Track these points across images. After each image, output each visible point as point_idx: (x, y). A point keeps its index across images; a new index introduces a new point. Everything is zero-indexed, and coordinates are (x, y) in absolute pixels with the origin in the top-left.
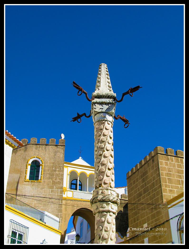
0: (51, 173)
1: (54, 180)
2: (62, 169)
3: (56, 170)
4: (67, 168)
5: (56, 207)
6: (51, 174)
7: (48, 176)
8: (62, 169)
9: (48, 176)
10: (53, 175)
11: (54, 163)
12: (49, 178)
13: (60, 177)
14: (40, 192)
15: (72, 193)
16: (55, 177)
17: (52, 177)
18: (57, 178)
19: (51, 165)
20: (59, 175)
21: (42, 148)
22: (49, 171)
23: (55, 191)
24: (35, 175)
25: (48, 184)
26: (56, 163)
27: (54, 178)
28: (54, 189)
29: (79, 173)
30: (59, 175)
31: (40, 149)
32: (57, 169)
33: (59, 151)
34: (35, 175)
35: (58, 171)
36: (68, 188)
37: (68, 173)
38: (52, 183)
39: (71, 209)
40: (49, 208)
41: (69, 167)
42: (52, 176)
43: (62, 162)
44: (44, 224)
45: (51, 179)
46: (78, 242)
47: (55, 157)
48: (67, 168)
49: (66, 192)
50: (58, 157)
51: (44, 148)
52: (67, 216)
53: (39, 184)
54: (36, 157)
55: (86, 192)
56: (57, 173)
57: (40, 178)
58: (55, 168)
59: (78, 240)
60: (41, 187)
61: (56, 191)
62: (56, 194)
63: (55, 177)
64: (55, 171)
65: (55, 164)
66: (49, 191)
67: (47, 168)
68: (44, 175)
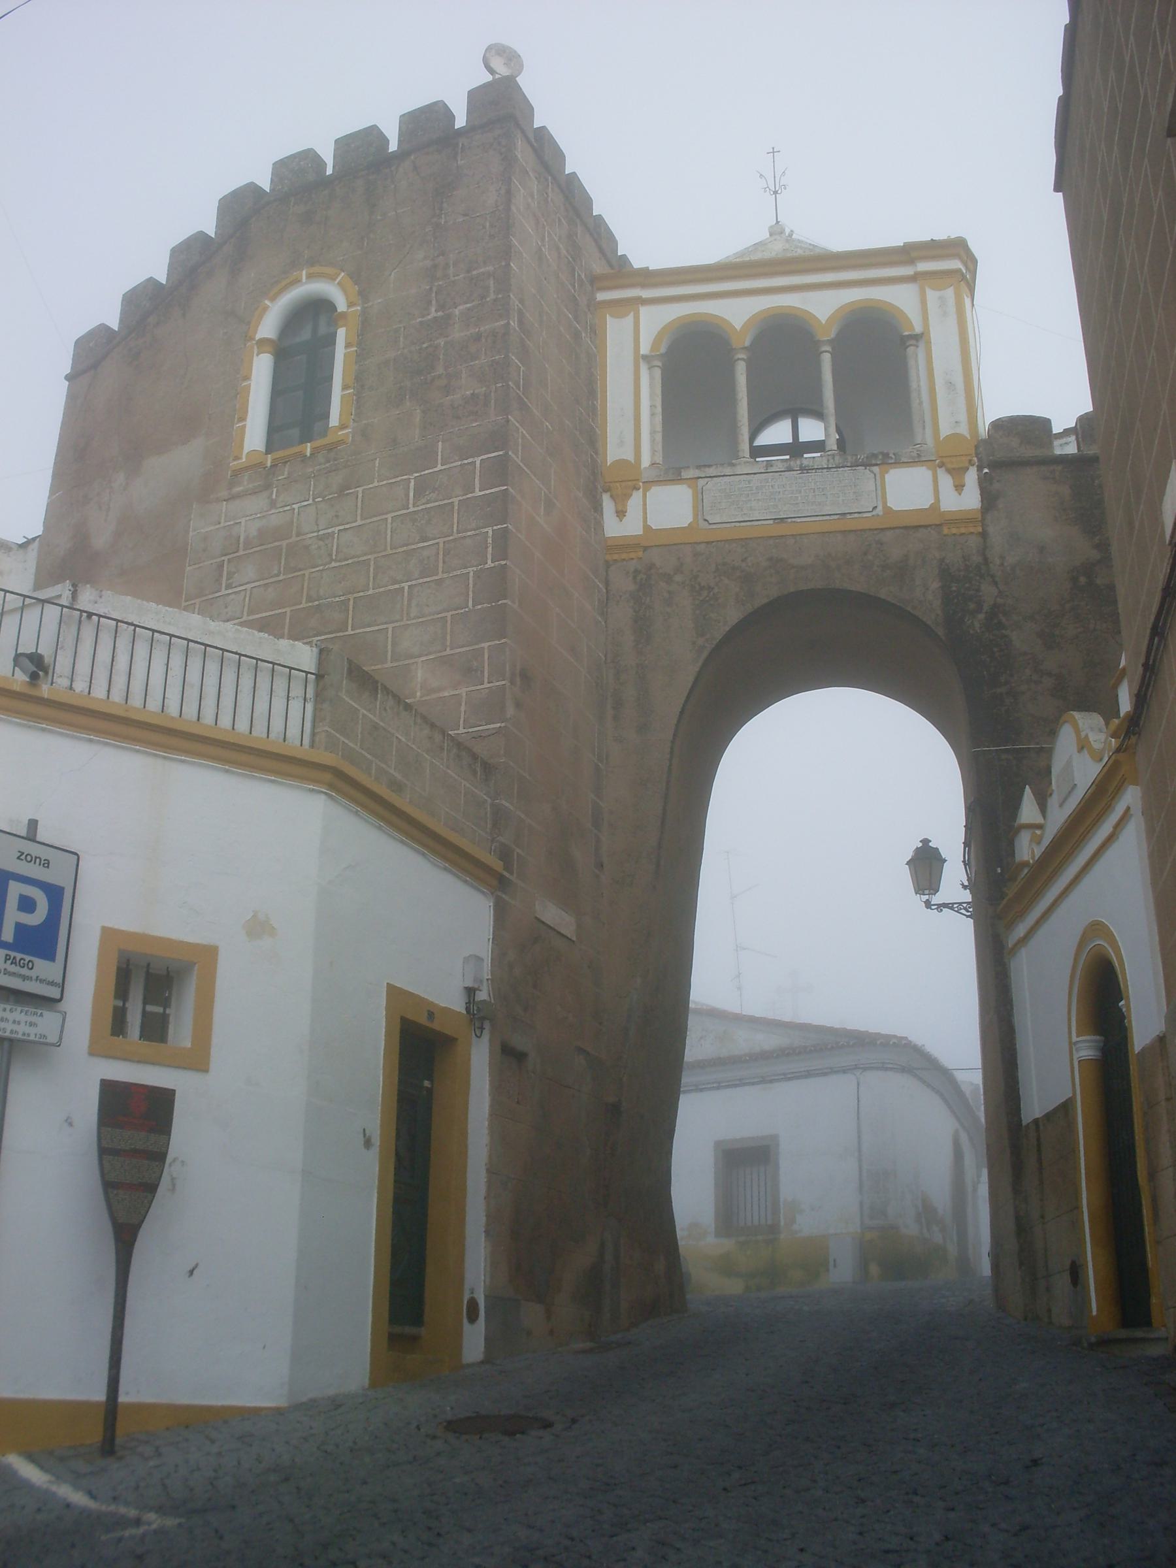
2: (492, 296)
8: (492, 296)
14: (337, 516)
15: (690, 491)
28: (439, 467)
32: (457, 312)
36: (659, 459)
40: (405, 622)
41: (644, 311)
46: (937, 899)
48: (630, 318)
49: (637, 496)
58: (441, 307)
62: (456, 500)
63: (440, 376)
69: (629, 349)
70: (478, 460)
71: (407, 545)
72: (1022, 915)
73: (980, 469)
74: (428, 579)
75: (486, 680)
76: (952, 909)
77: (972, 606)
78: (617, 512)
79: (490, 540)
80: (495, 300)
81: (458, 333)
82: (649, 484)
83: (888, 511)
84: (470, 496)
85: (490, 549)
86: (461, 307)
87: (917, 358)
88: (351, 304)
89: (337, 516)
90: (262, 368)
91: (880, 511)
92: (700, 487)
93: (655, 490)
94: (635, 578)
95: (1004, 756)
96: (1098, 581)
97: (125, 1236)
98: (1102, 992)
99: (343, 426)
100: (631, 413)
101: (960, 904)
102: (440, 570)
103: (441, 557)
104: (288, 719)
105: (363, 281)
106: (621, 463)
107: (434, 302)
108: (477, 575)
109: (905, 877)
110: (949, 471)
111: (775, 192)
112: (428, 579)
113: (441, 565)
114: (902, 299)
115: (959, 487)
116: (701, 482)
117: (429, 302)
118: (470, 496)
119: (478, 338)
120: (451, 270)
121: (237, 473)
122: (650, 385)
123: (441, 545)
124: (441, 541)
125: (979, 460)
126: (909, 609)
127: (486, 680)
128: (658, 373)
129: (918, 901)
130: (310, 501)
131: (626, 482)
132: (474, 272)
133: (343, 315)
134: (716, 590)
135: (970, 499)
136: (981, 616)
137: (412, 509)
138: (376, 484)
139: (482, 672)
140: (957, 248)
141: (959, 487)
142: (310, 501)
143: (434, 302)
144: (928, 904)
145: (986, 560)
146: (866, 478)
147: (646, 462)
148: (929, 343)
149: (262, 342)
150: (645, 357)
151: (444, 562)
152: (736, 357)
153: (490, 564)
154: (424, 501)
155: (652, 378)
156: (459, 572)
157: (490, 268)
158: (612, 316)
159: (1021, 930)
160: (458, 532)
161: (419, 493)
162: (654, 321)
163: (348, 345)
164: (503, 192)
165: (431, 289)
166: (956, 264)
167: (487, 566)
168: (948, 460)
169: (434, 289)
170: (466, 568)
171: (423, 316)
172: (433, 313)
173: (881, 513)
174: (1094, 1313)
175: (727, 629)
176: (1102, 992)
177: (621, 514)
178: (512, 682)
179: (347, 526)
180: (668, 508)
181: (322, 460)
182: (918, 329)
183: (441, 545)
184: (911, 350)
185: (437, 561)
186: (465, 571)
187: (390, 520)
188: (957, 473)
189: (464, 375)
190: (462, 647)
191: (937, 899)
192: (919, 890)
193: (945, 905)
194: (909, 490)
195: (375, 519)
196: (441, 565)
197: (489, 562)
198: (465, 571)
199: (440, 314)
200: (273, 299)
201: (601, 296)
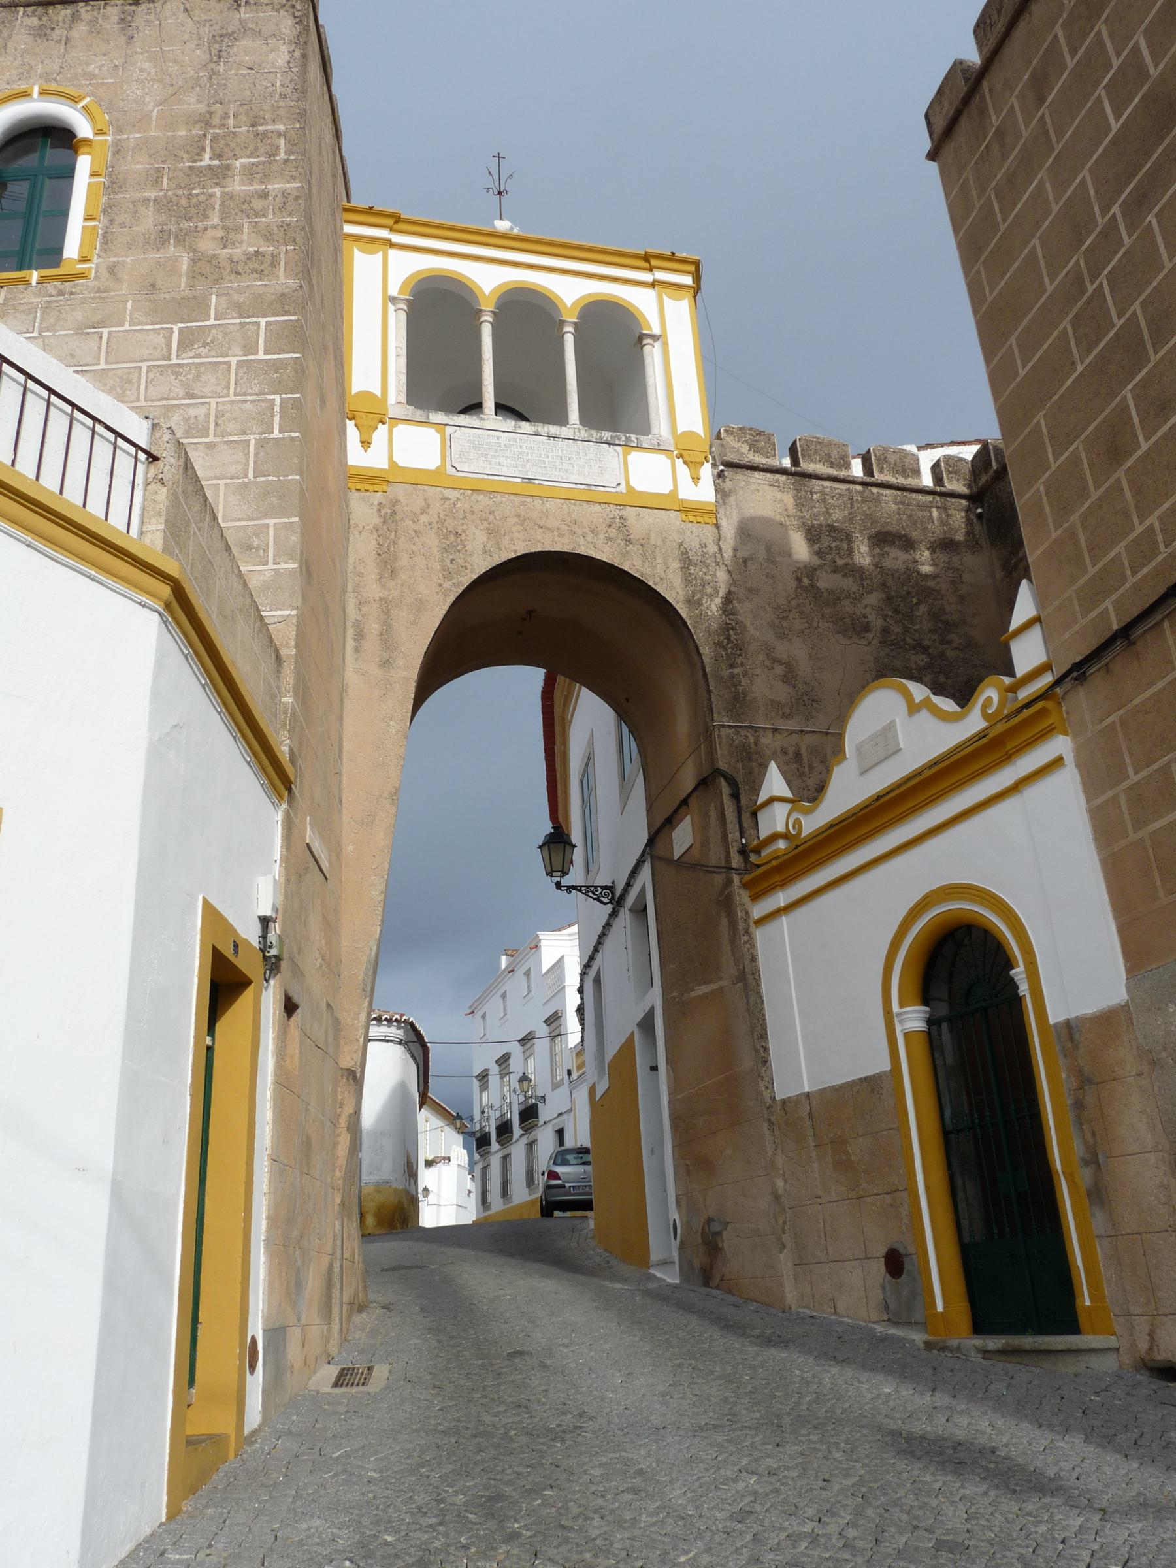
0: (180, 192)
1: (207, 245)
3: (228, 167)
4: (381, 253)
5: (233, 470)
6: (184, 202)
7: (149, 220)
8: (283, 156)
11: (206, 120)
12: (162, 238)
14: (72, 356)
15: (438, 436)
16: (215, 220)
17: (185, 225)
18: (238, 229)
19: (182, 133)
20: (258, 204)
21: (92, 22)
22: (157, 181)
23: (220, 336)
25: (153, 285)
26: (226, 116)
27: (211, 233)
29: (487, 291)
30: (258, 204)
31: (81, 28)
32: (238, 164)
33: (250, 25)
35: (250, 173)
36: (403, 398)
37: (393, 291)
38: (193, 276)
39: (437, 566)
41: (392, 253)
42: (189, 219)
43: (281, 104)
46: (566, 881)
47: (213, 74)
49: (382, 429)
50: (245, 72)
51: (115, 19)
52: (401, 617)
53: (61, 293)
54: (43, 92)
55: (564, 431)
56: (237, 186)
57: (72, 248)
58: (217, 156)
59: (564, 873)
60: (79, 316)
61: (226, 334)
62: (234, 361)
63: (215, 227)
64: (220, 174)
65: (216, 120)
66: (160, 340)
67: (136, 165)
68: (111, 221)
70: (263, 322)
71: (167, 399)
72: (783, 884)
73: (714, 465)
74: (196, 440)
75: (271, 560)
76: (580, 891)
77: (709, 590)
78: (362, 442)
79: (277, 409)
80: (286, 161)
81: (237, 186)
83: (630, 489)
84: (252, 357)
85: (277, 419)
86: (243, 160)
87: (653, 353)
88: (100, 132)
89: (72, 356)
91: (623, 488)
92: (448, 434)
93: (401, 430)
94: (379, 510)
95: (742, 733)
96: (821, 584)
99: (84, 259)
100: (376, 351)
101: (588, 887)
102: (211, 432)
103: (212, 418)
106: (366, 395)
107: (208, 149)
108: (261, 445)
109: (536, 861)
110: (685, 462)
111: (500, 193)
112: (196, 440)
113: (212, 426)
115: (696, 479)
116: (449, 430)
117: (203, 149)
118: (252, 357)
119: (264, 195)
120: (231, 121)
122: (398, 323)
123: (213, 406)
124: (213, 401)
125: (714, 458)
126: (650, 584)
127: (271, 560)
128: (403, 316)
129: (549, 883)
130: (35, 334)
131: (372, 415)
132: (260, 128)
134: (463, 537)
136: (718, 601)
137: (174, 361)
138: (127, 327)
139: (266, 551)
141: (696, 479)
142: (35, 334)
143: (208, 149)
144: (558, 886)
145: (720, 549)
146: (612, 456)
147: (392, 398)
148: (665, 345)
150: (393, 300)
151: (216, 424)
152: (483, 319)
153: (276, 434)
154: (192, 354)
155: (398, 320)
156: (236, 438)
157: (282, 128)
158: (361, 250)
159: (781, 898)
160: (236, 394)
161: (184, 345)
163: (94, 174)
164: (297, 54)
165: (205, 135)
167: (272, 436)
169: (209, 136)
170: (245, 433)
171: (195, 161)
172: (206, 160)
173: (624, 491)
174: (940, 1308)
175: (475, 577)
177: (366, 443)
178: (300, 567)
179: (85, 368)
181: (54, 292)
182: (656, 330)
183: (213, 406)
184: (647, 349)
185: (208, 422)
186: (243, 437)
187: (144, 370)
188: (694, 466)
189: (245, 230)
190: (239, 520)
191: (566, 881)
192: (550, 874)
193: (574, 888)
194: (650, 472)
195: (125, 365)
196: (212, 426)
197: (276, 431)
198: (243, 437)
199: (216, 162)
201: (348, 229)
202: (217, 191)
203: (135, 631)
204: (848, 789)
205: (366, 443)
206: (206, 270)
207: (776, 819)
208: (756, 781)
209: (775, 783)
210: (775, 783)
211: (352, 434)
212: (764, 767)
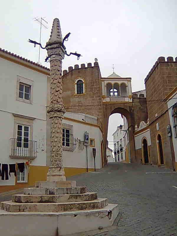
1: (93, 92)
7: (89, 90)
9: (89, 90)
10: (92, 89)
13: (97, 89)
24: (80, 90)
34: (80, 90)
41: (105, 81)
44: (84, 122)
45: (92, 91)
46: (122, 130)
49: (105, 99)
57: (84, 92)
59: (122, 129)
64: (93, 85)
69: (104, 84)
82: (106, 98)
88: (84, 81)
90: (76, 85)
97: (95, 158)
98: (145, 141)
99: (85, 93)
104: (95, 123)
105: (85, 79)
114: (126, 82)
115: (131, 99)
121: (75, 96)
133: (84, 83)
135: (131, 101)
140: (130, 78)
149: (76, 84)
159: (136, 136)
162: (106, 82)
166: (130, 80)
168: (129, 97)
176: (145, 141)
177: (104, 100)
180: (108, 100)
188: (130, 98)
191: (122, 130)
194: (127, 100)
200: (77, 79)
201: (101, 80)
202: (94, 87)
203: (99, 129)
204: (140, 129)
205: (104, 100)
206: (94, 94)
207: (136, 129)
208: (135, 126)
209: (136, 126)
210: (136, 126)
211: (103, 99)
212: (135, 125)
